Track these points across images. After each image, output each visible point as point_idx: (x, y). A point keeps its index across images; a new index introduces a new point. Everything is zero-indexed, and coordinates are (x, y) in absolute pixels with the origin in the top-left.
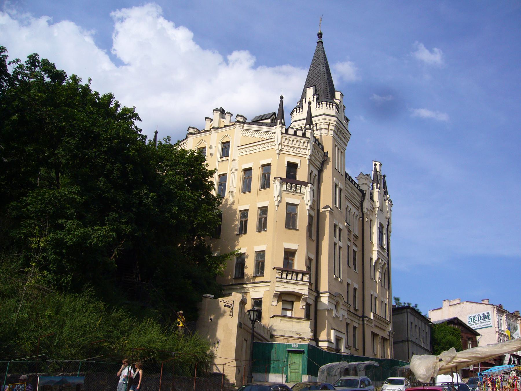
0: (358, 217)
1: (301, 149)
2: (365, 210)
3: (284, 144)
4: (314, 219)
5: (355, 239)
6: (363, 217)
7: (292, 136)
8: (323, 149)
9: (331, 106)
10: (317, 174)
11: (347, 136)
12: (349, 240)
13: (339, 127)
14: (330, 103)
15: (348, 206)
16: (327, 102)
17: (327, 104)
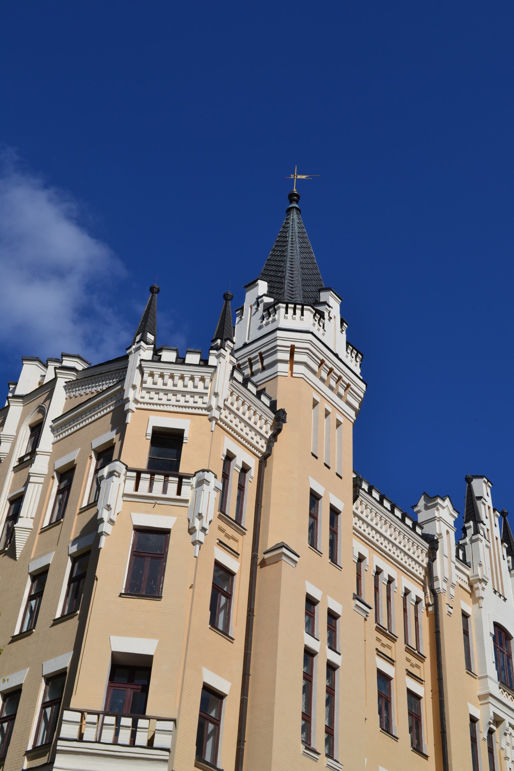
0: (423, 604)
1: (193, 394)
2: (440, 585)
3: (144, 385)
4: (236, 578)
5: (414, 661)
6: (436, 605)
7: (172, 365)
8: (273, 406)
9: (298, 312)
10: (253, 463)
11: (352, 386)
12: (391, 661)
13: (322, 357)
14: (295, 304)
15: (379, 572)
16: (287, 304)
17: (287, 309)
